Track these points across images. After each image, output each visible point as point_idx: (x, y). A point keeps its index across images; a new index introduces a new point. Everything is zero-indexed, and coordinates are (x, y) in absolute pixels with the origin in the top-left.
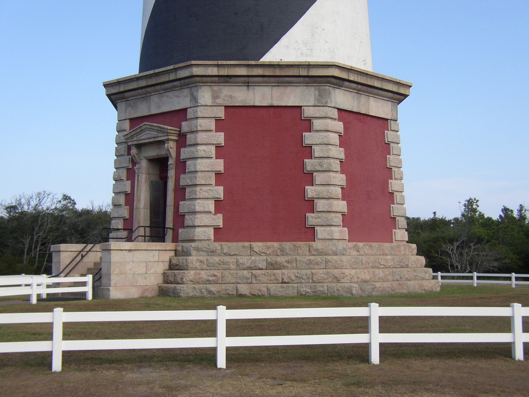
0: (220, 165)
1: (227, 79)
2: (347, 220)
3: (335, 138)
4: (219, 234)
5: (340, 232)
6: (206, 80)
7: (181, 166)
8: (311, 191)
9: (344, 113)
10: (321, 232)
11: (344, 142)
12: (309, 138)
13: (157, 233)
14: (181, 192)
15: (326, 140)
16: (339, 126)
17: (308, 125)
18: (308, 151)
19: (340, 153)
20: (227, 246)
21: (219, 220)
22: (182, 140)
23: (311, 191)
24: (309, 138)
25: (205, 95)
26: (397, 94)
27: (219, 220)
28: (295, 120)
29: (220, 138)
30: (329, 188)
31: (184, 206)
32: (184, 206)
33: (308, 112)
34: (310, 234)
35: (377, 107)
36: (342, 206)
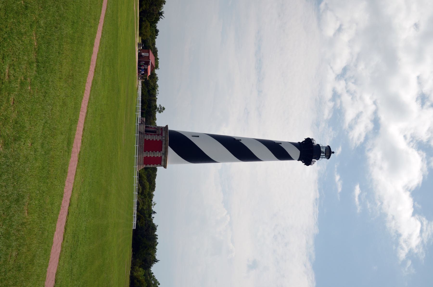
0: (155, 140)
1: (166, 141)
2: (147, 157)
3: (158, 155)
4: (145, 140)
5: (145, 156)
6: (166, 138)
7: (155, 135)
8: (151, 152)
9: (161, 157)
10: (145, 153)
11: (158, 157)
12: (158, 152)
13: (146, 131)
14: (151, 135)
15: (158, 154)
16: (159, 156)
17: (160, 152)
18: (156, 152)
19: (156, 156)
20: (144, 140)
21: (147, 139)
22: (158, 135)
23: (151, 152)
24: (158, 152)
25: (164, 138)
26: (165, 167)
27: (147, 139)
28: (160, 150)
29: (158, 140)
30: (151, 154)
31: (149, 135)
32: (149, 135)
33: (161, 152)
34: (145, 151)
35: (163, 163)
36: (149, 156)
